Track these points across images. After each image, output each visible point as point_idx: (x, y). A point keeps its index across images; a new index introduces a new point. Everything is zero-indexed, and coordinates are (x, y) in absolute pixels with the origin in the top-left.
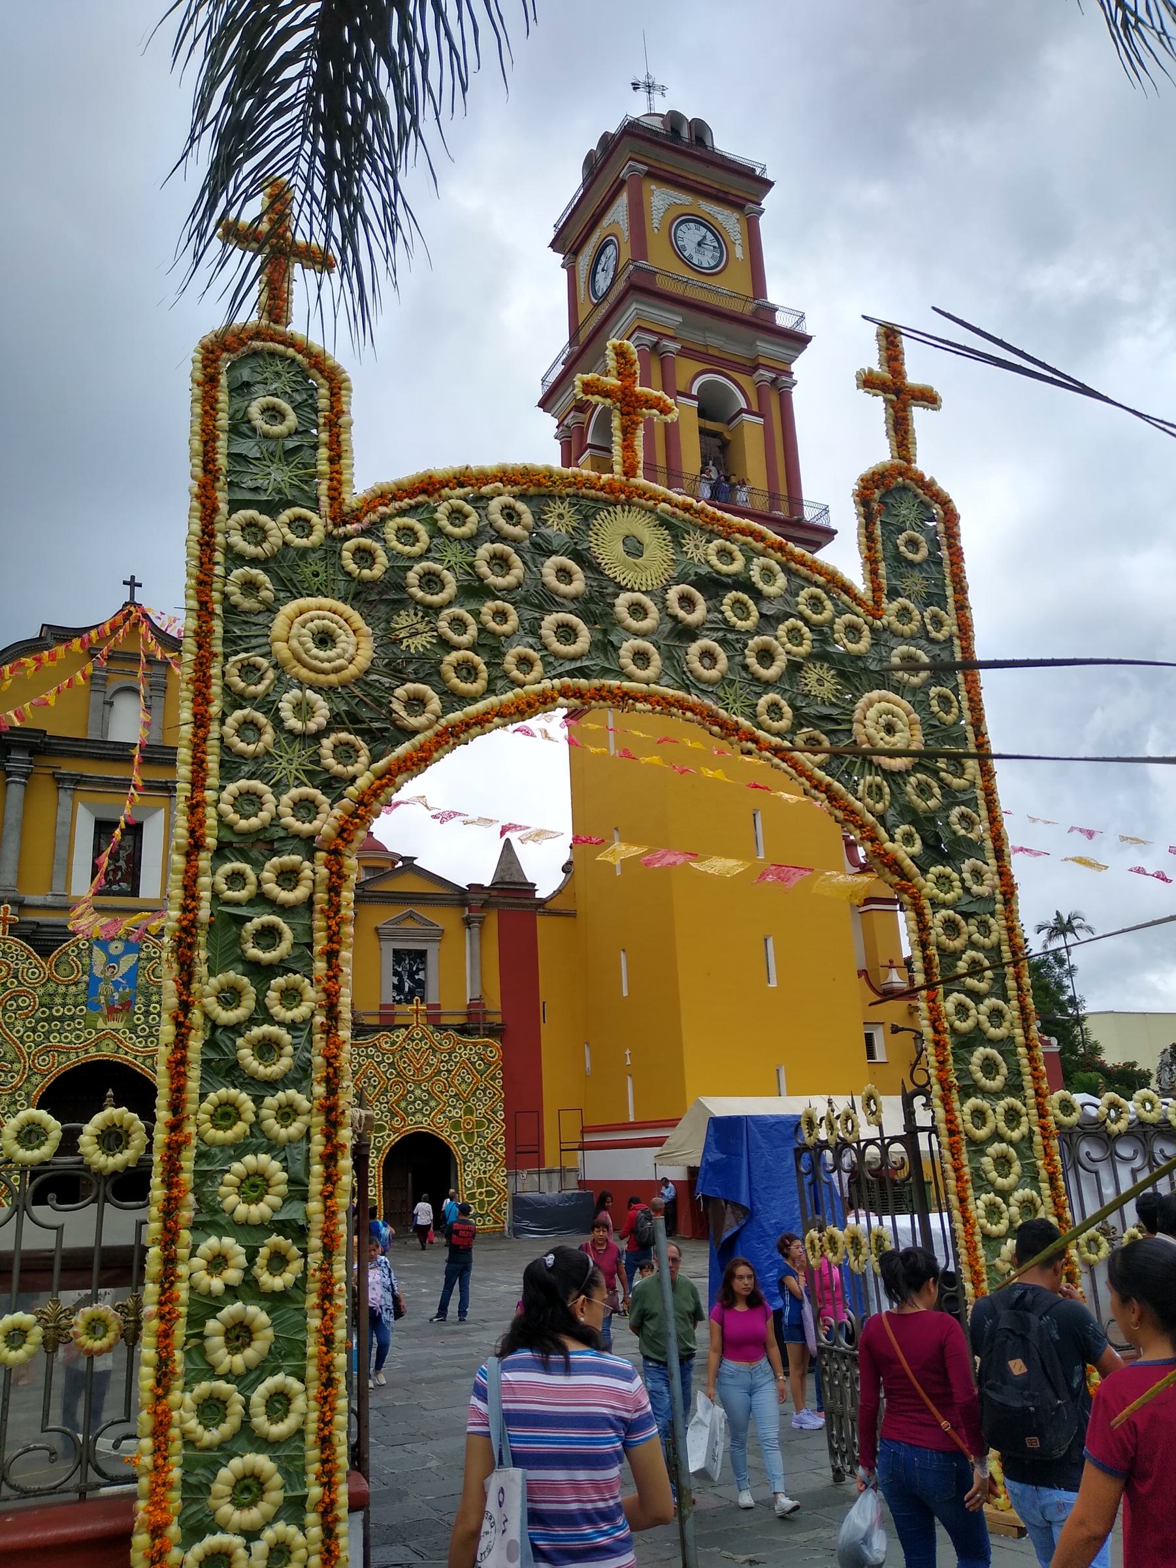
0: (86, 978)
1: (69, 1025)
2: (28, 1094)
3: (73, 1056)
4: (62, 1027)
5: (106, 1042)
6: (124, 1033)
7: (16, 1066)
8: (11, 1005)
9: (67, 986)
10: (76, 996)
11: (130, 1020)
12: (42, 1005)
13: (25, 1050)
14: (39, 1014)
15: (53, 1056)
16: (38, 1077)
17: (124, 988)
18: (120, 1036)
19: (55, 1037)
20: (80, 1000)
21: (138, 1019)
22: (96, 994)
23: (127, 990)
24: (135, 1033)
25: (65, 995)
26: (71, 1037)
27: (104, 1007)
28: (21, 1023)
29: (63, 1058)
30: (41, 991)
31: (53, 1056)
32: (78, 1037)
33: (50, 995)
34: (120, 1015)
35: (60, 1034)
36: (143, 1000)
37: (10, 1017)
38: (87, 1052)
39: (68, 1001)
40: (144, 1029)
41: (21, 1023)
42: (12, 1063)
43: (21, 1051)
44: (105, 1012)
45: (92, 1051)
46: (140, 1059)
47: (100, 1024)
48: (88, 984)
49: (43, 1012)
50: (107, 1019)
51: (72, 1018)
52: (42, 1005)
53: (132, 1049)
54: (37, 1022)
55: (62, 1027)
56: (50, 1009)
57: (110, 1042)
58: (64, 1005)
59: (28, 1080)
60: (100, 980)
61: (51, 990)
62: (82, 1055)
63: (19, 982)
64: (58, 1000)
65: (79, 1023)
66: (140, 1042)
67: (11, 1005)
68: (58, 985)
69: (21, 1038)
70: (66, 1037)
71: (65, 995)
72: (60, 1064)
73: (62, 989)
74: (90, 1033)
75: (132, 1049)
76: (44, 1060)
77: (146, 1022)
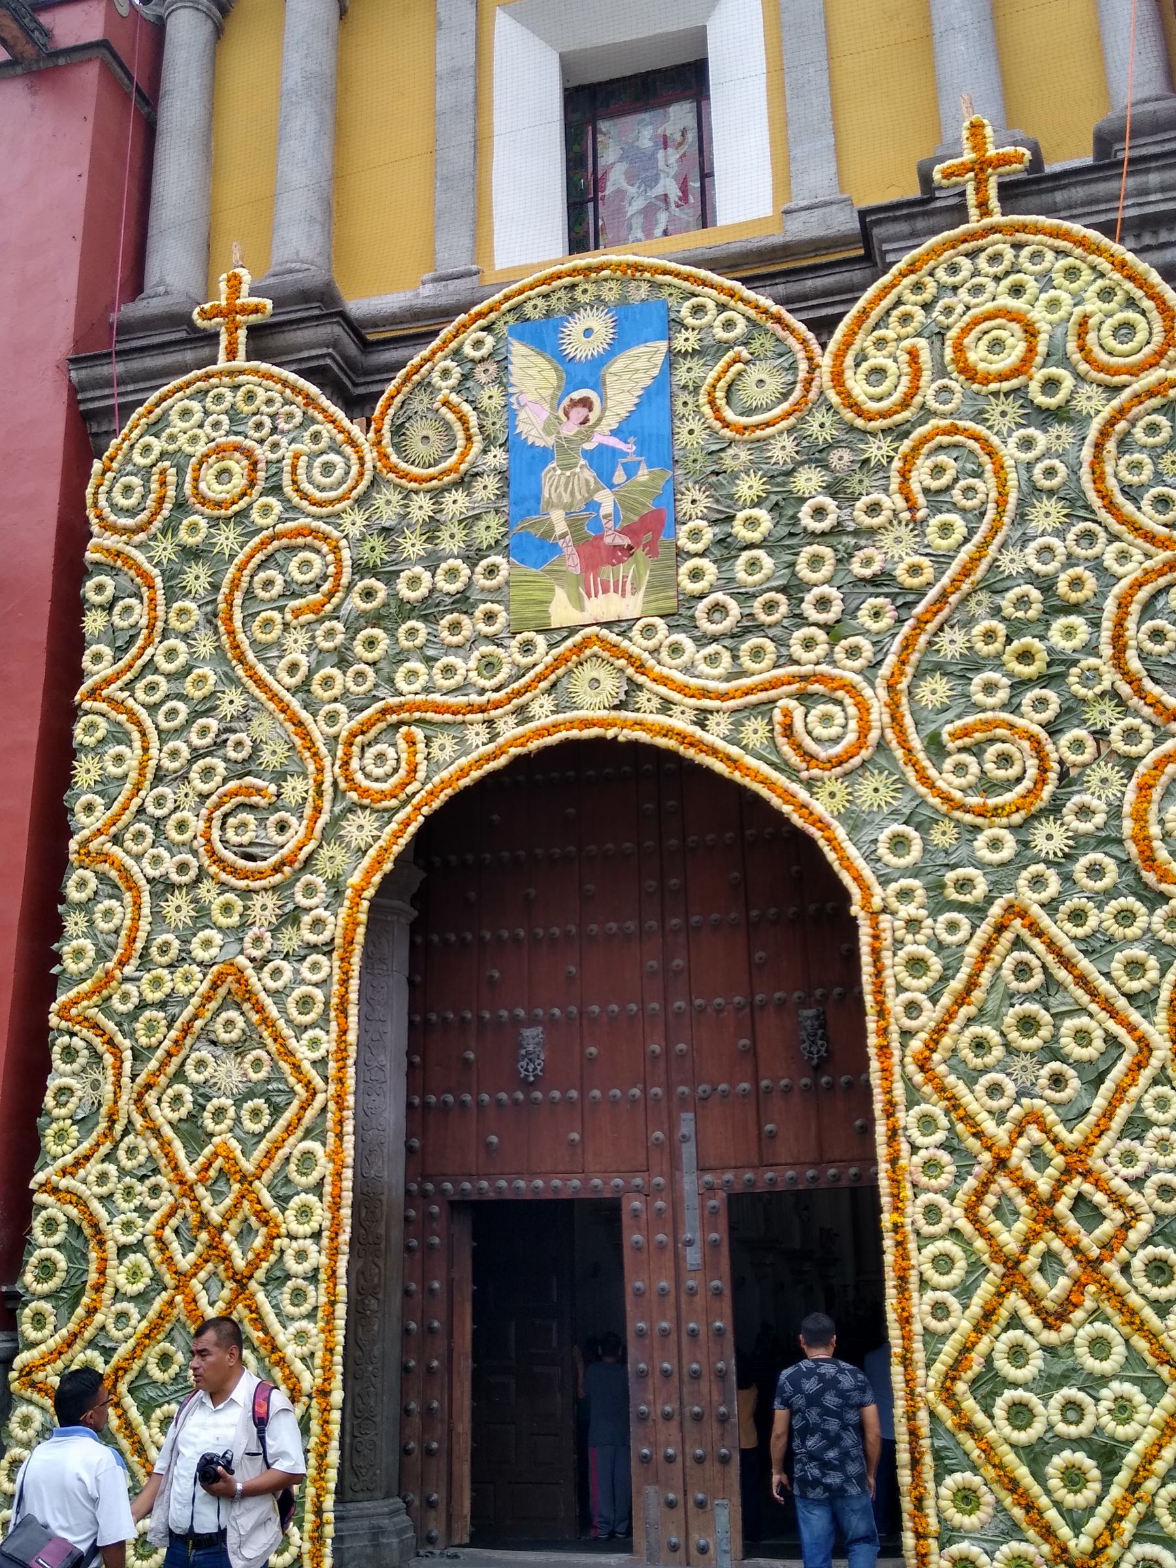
0: (497, 458)
1: (455, 627)
2: (336, 888)
3: (476, 735)
4: (433, 636)
5: (589, 671)
6: (649, 631)
7: (295, 788)
8: (268, 584)
9: (437, 494)
10: (469, 522)
11: (663, 583)
12: (361, 569)
13: (318, 730)
14: (356, 602)
15: (412, 743)
16: (366, 819)
17: (631, 471)
18: (637, 645)
19: (413, 673)
20: (484, 535)
21: (696, 575)
22: (533, 501)
23: (643, 475)
24: (690, 626)
25: (432, 529)
26: (465, 666)
27: (568, 547)
28: (302, 637)
29: (445, 744)
30: (354, 523)
31: (412, 743)
32: (489, 666)
33: (386, 531)
34: (626, 569)
35: (429, 661)
36: (704, 502)
37: (268, 624)
38: (522, 714)
39: (451, 542)
40: (719, 608)
41: (302, 637)
42: (280, 777)
43: (306, 735)
44: (573, 563)
45: (542, 709)
46: (719, 726)
47: (562, 612)
48: (502, 474)
49: (368, 594)
50: (584, 588)
51: (463, 602)
52: (361, 569)
53: (683, 689)
54: (352, 631)
55: (433, 636)
56: (390, 578)
57: (602, 673)
58: (432, 562)
59: (332, 833)
60: (543, 456)
61: (388, 516)
62: (509, 729)
63: (289, 507)
64: (413, 545)
65: (490, 617)
66: (712, 660)
67: (268, 584)
68: (407, 495)
69: (304, 688)
70: (449, 670)
71: (432, 529)
72: (437, 766)
73: (422, 507)
74: (527, 648)
75: (683, 689)
76: (380, 757)
77: (727, 583)
